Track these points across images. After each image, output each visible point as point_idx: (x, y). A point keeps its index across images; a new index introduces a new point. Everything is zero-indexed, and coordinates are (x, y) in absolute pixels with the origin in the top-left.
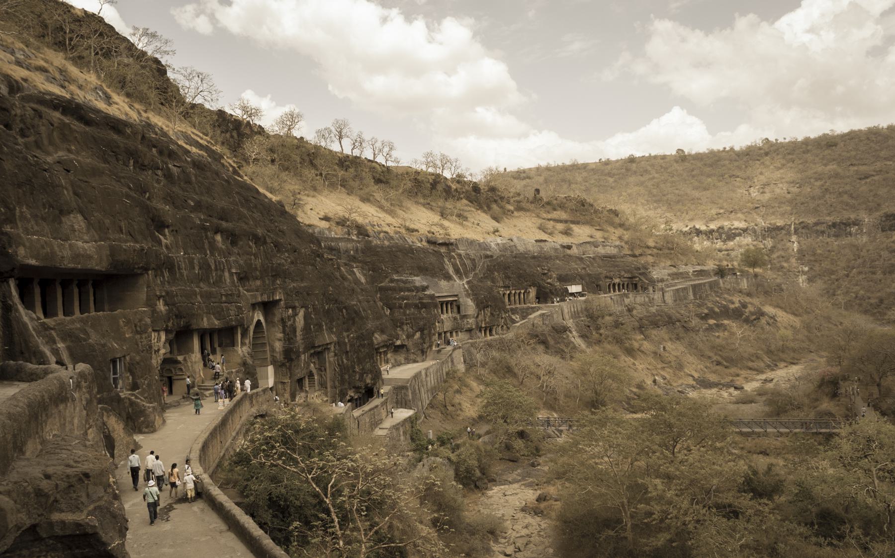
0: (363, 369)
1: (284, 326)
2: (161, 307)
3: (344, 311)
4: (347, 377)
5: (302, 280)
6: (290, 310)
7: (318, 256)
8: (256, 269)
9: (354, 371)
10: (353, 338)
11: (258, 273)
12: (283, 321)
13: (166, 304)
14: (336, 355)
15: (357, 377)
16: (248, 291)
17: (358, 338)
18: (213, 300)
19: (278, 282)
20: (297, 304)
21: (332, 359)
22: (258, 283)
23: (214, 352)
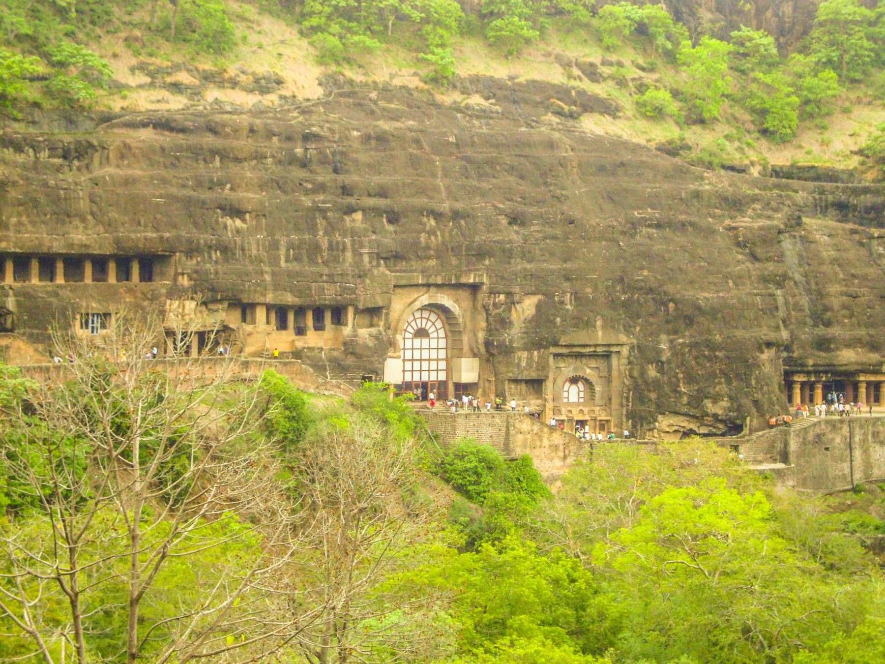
0: (699, 391)
1: (488, 314)
2: (184, 281)
3: (671, 305)
4: (653, 396)
5: (565, 261)
6: (502, 297)
7: (658, 226)
8: (428, 248)
9: (676, 391)
10: (684, 343)
11: (432, 252)
12: (486, 308)
13: (190, 279)
14: (630, 363)
15: (685, 400)
16: (391, 271)
17: (693, 346)
18: (299, 279)
19: (487, 262)
20: (517, 289)
21: (623, 368)
22: (432, 263)
23: (319, 326)
